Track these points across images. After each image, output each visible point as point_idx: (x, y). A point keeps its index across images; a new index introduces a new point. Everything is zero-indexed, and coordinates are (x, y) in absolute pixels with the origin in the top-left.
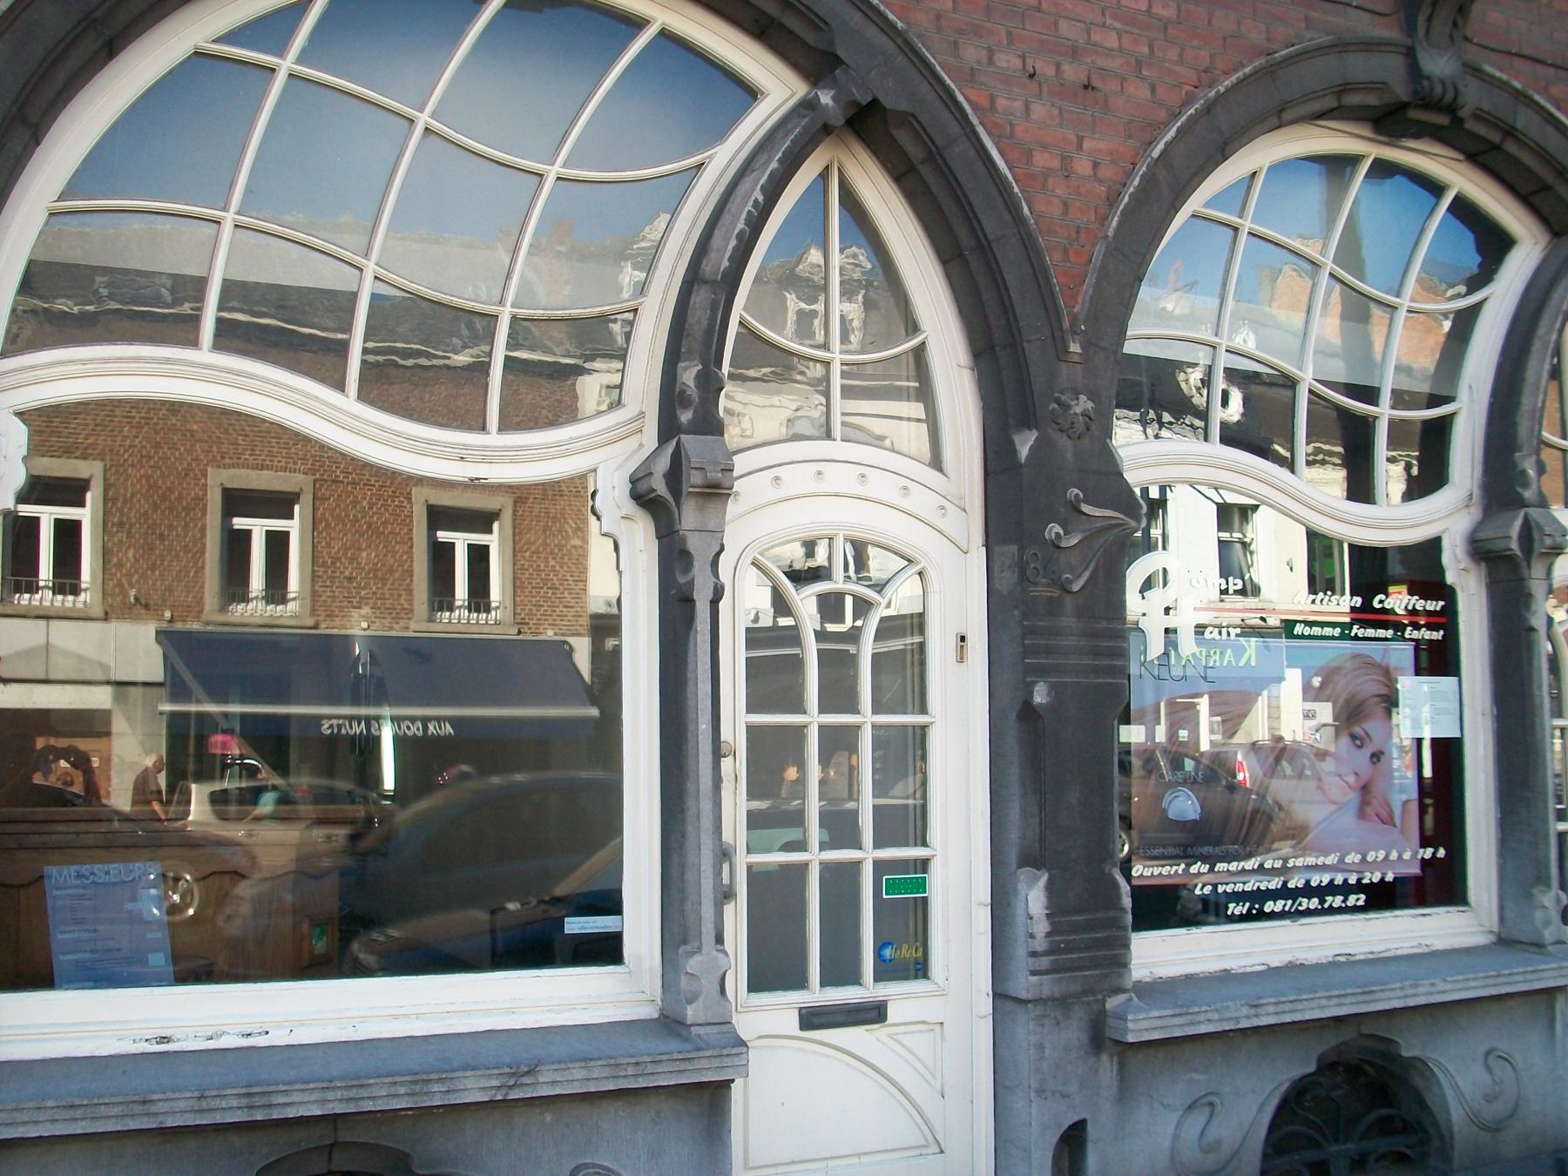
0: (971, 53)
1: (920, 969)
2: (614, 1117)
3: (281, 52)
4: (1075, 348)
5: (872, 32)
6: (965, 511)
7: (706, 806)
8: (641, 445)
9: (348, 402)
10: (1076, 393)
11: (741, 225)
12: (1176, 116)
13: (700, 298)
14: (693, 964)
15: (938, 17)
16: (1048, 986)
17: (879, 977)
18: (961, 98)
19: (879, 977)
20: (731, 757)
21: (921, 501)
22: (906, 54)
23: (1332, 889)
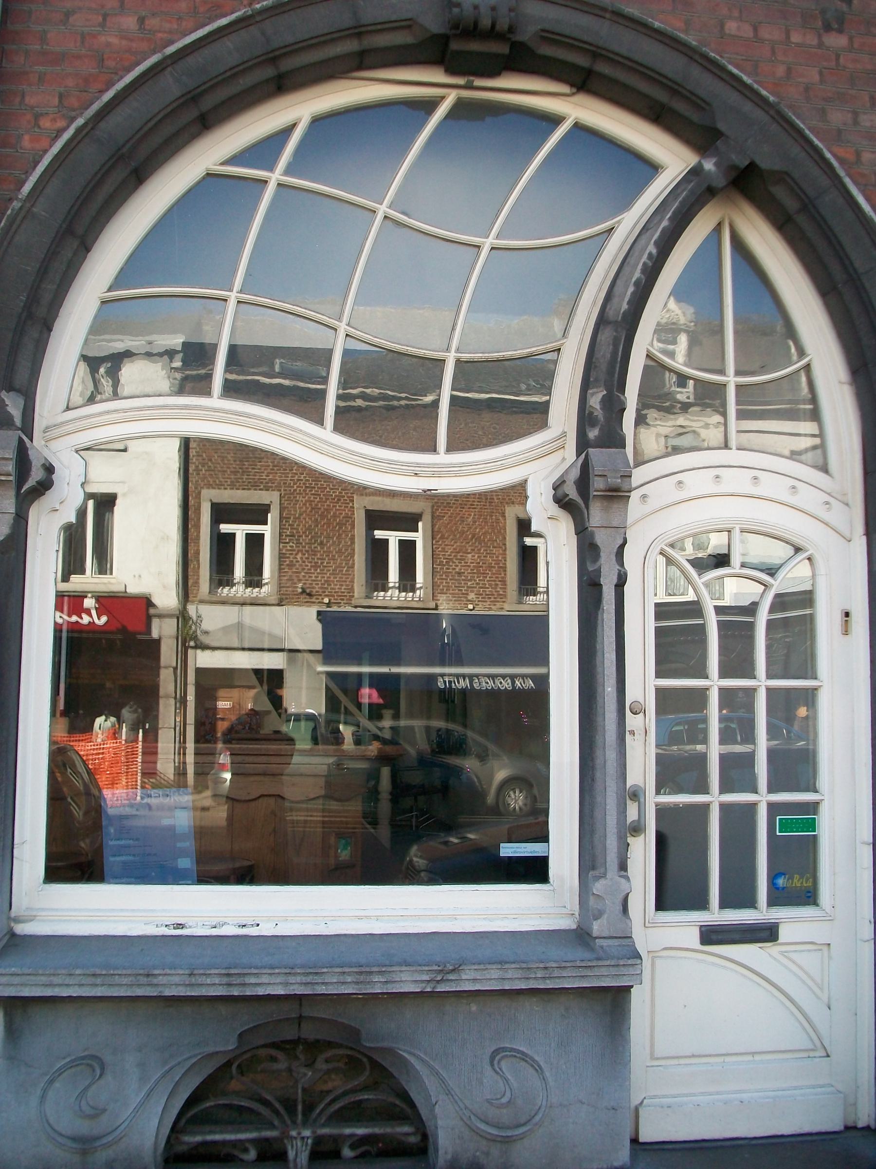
0: (837, 117)
3: (271, 168)
5: (748, 107)
6: (847, 504)
7: (611, 755)
8: (564, 459)
9: (326, 433)
11: (637, 274)
13: (607, 335)
14: (598, 887)
15: (807, 89)
17: (773, 902)
18: (828, 155)
19: (773, 902)
20: (642, 714)
21: (809, 498)
22: (778, 123)
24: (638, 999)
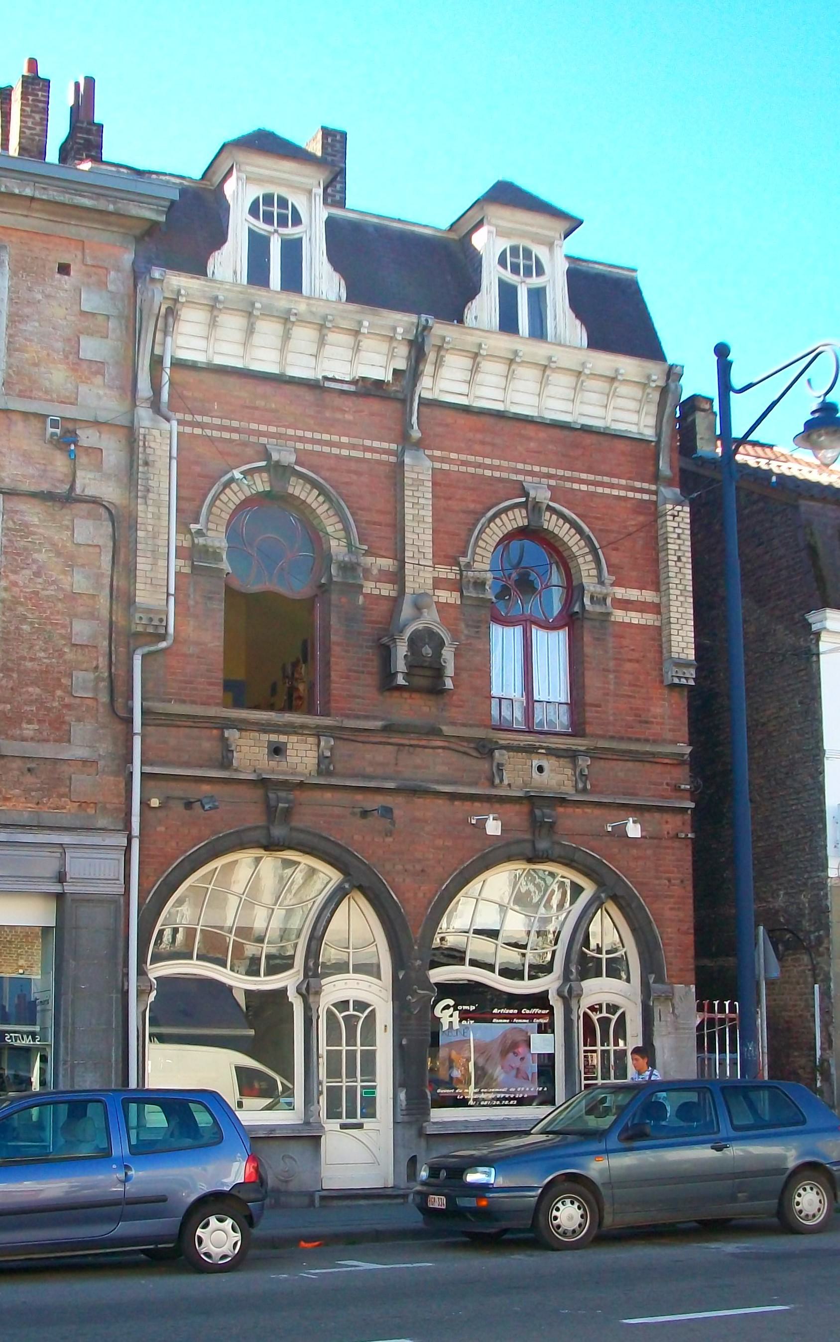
0: (388, 866)
1: (373, 1116)
2: (292, 1143)
4: (416, 948)
7: (315, 1070)
8: (299, 979)
10: (416, 960)
11: (324, 923)
12: (451, 875)
14: (312, 1108)
16: (406, 1118)
17: (361, 1117)
18: (384, 881)
19: (361, 1117)
21: (375, 989)
23: (505, 1099)
24: (323, 1139)
